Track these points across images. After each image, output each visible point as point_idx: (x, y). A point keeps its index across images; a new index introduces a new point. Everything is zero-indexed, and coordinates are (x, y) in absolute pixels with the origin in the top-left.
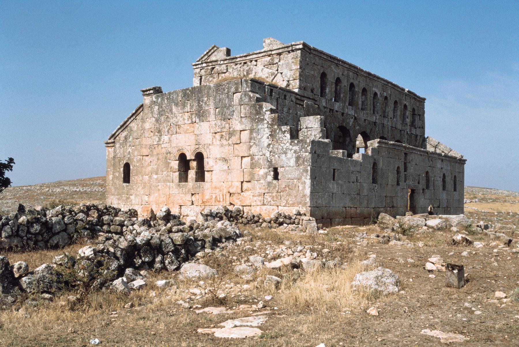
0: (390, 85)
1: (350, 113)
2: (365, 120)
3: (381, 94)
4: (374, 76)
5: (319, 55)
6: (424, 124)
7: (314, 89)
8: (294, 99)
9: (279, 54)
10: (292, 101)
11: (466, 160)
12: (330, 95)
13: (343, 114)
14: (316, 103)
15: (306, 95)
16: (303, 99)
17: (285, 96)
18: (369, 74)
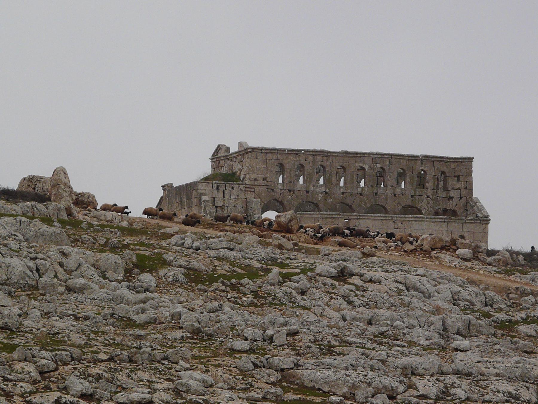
0: (385, 156)
1: (317, 189)
2: (343, 193)
3: (370, 167)
4: (357, 153)
5: (272, 151)
6: (471, 184)
7: (266, 178)
8: (244, 189)
9: (243, 155)
10: (241, 190)
11: (490, 220)
12: (288, 179)
13: (308, 192)
14: (270, 187)
15: (256, 184)
16: (252, 187)
17: (233, 188)
18: (347, 153)
